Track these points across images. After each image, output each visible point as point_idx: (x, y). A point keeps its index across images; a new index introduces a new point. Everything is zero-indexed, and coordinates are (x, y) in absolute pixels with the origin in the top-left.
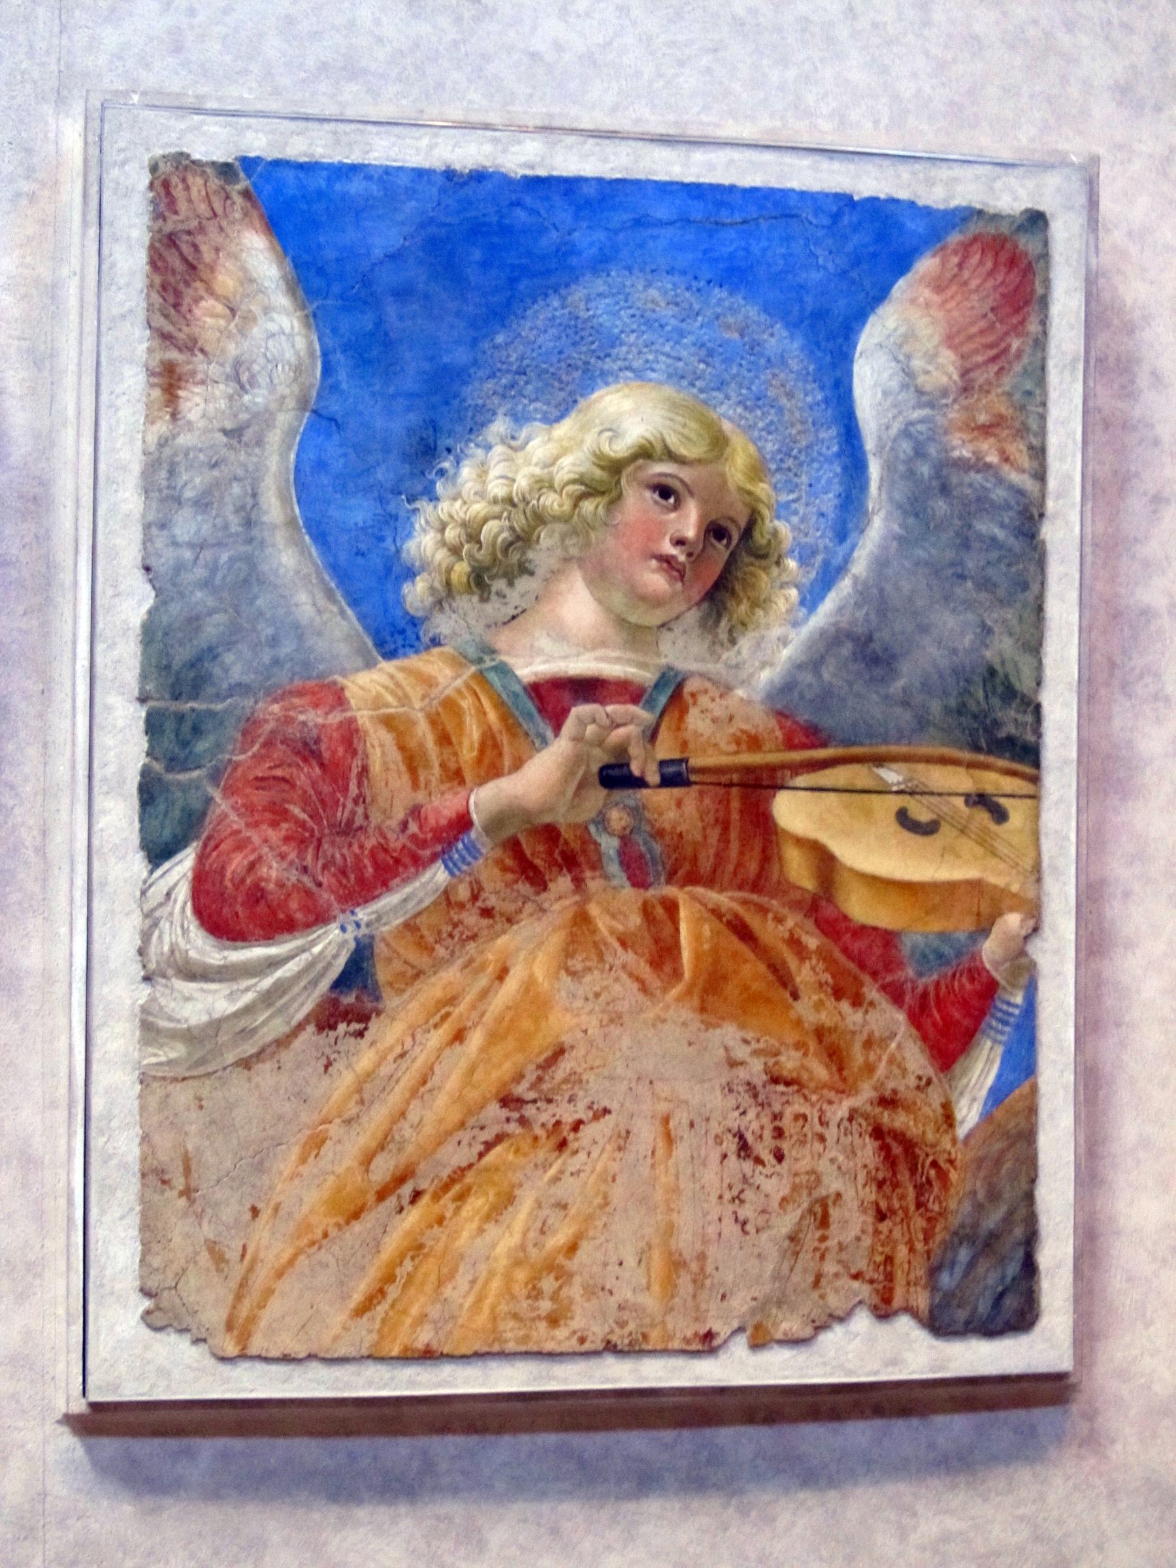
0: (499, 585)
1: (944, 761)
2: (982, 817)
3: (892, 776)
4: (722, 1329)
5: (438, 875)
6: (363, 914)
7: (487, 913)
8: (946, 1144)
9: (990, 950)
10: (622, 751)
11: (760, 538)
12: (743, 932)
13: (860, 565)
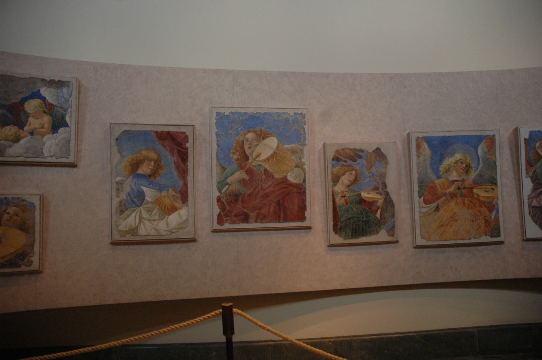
0: (448, 172)
1: (489, 185)
2: (492, 190)
3: (484, 187)
4: (471, 237)
5: (444, 198)
6: (438, 202)
7: (448, 201)
8: (491, 220)
9: (494, 202)
10: (459, 186)
11: (471, 166)
12: (471, 202)
13: (480, 168)
